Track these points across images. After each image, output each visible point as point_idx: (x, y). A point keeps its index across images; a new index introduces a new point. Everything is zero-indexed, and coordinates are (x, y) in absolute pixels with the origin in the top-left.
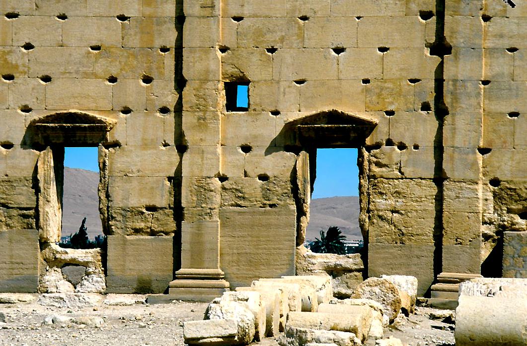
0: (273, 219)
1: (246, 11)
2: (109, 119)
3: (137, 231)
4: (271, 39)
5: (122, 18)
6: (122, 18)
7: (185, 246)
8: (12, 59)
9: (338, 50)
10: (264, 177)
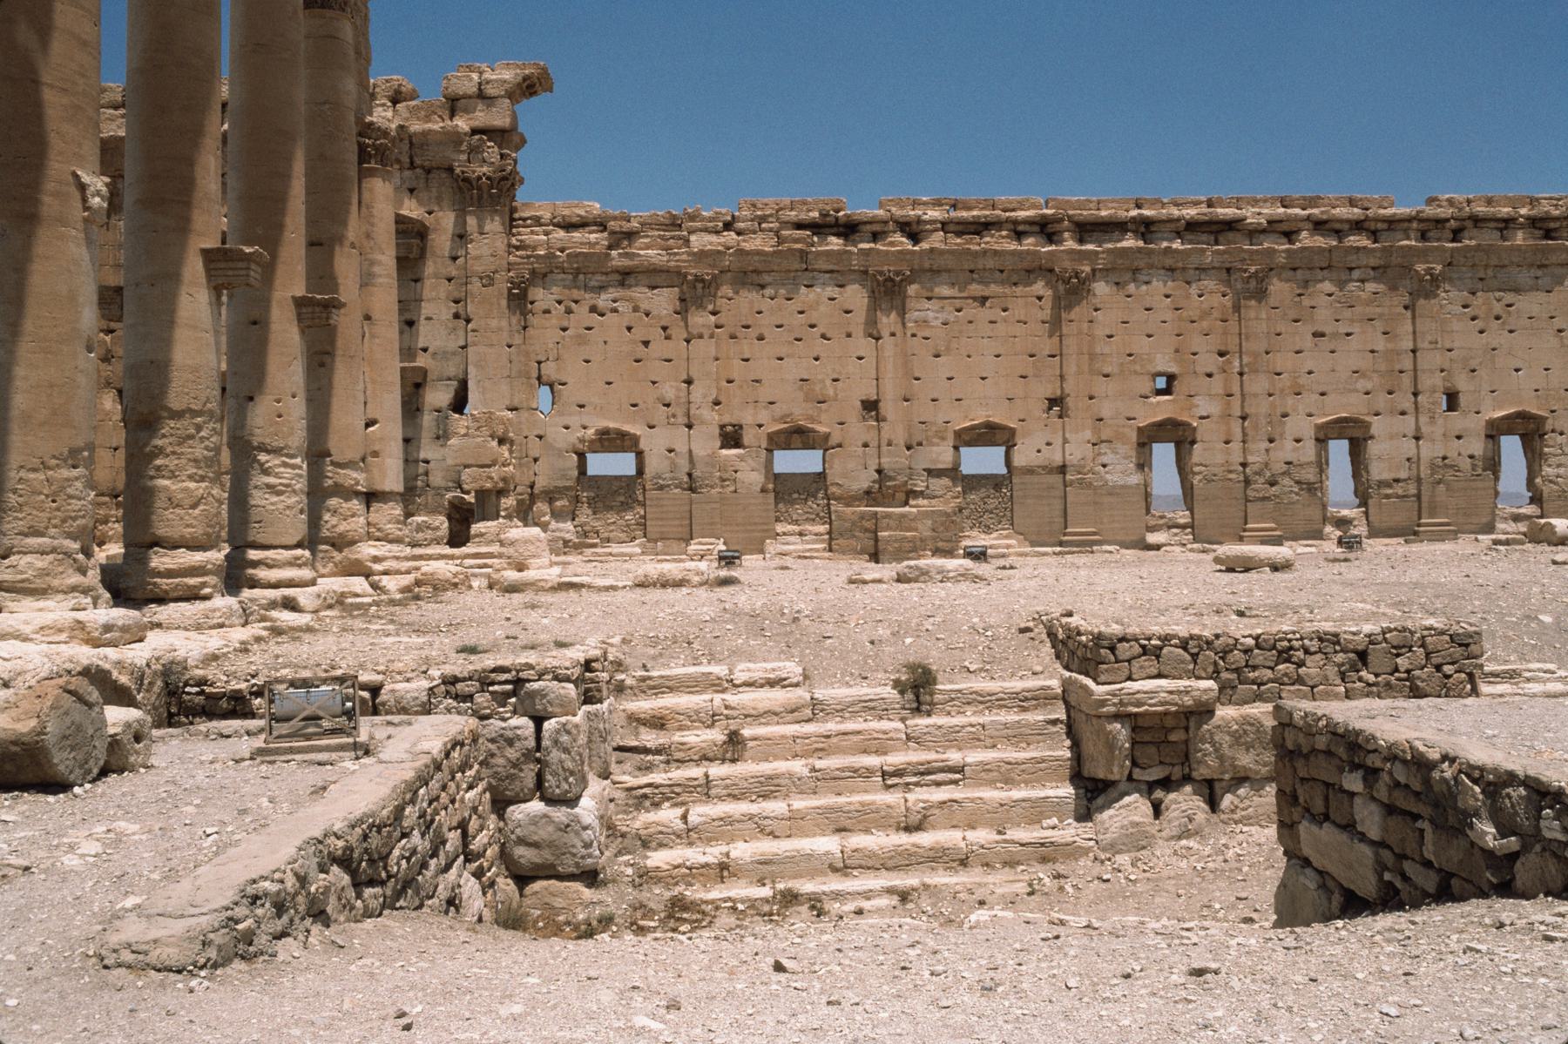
0: (1479, 484)
1: (1456, 345)
2: (1367, 419)
3: (1387, 496)
4: (1473, 364)
5: (1372, 351)
6: (1372, 351)
7: (1424, 505)
8: (1301, 381)
9: (1517, 370)
10: (1471, 457)
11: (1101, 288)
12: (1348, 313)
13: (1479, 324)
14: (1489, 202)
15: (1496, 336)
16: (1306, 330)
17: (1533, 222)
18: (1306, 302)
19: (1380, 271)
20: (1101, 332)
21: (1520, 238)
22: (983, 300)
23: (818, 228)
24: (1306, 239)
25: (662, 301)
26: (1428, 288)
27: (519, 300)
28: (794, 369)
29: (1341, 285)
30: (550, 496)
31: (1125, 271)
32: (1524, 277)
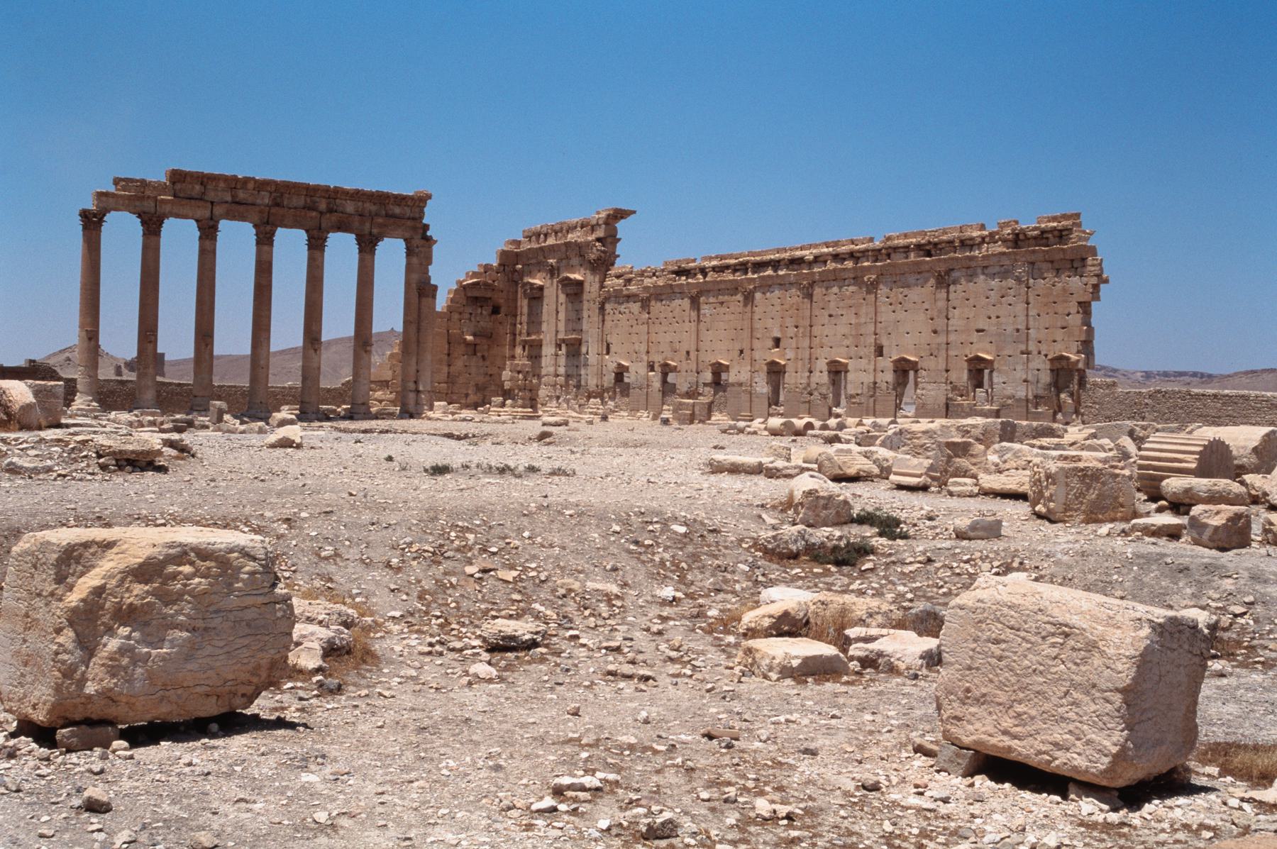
11: (758, 295)
12: (841, 304)
13: (892, 308)
14: (906, 236)
15: (901, 315)
16: (826, 313)
17: (919, 247)
18: (827, 298)
19: (857, 280)
20: (756, 317)
21: (912, 256)
22: (722, 303)
23: (680, 272)
24: (831, 265)
25: (635, 307)
26: (872, 287)
27: (602, 309)
28: (668, 337)
29: (840, 288)
30: (607, 390)
31: (766, 286)
32: (911, 279)
